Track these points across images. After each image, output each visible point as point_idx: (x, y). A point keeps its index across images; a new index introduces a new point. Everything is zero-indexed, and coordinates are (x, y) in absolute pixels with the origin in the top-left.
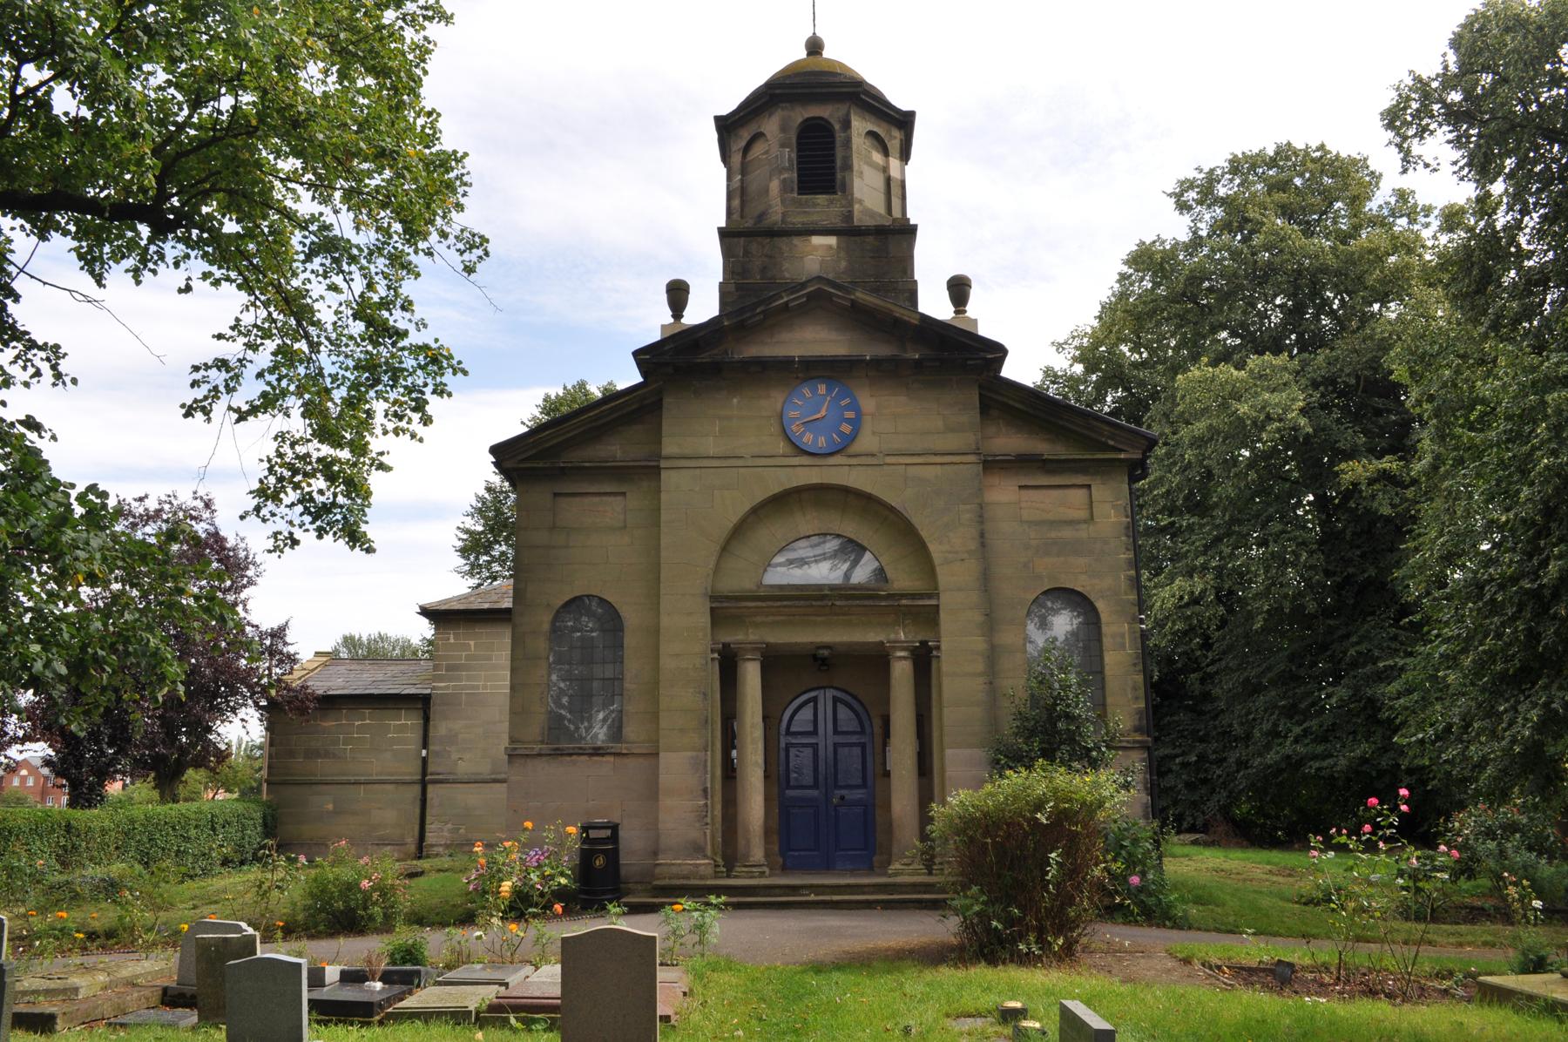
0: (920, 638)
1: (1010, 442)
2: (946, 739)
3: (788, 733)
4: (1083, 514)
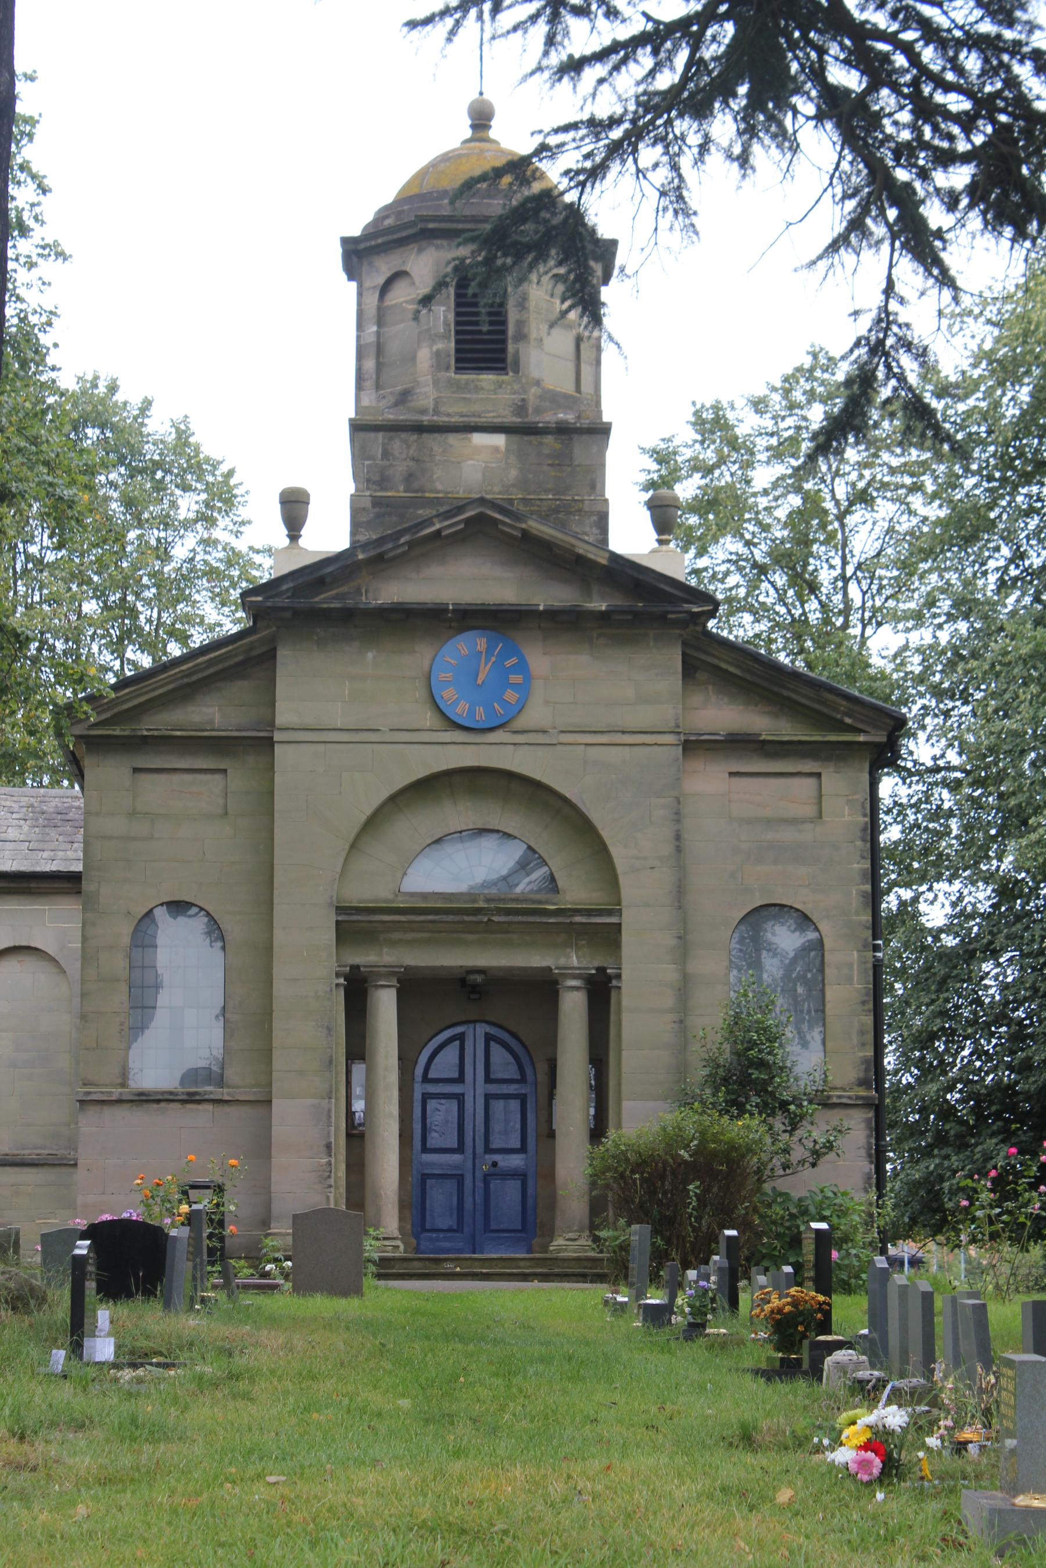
0: (596, 964)
1: (721, 714)
2: (624, 1088)
3: (426, 1079)
4: (810, 811)
